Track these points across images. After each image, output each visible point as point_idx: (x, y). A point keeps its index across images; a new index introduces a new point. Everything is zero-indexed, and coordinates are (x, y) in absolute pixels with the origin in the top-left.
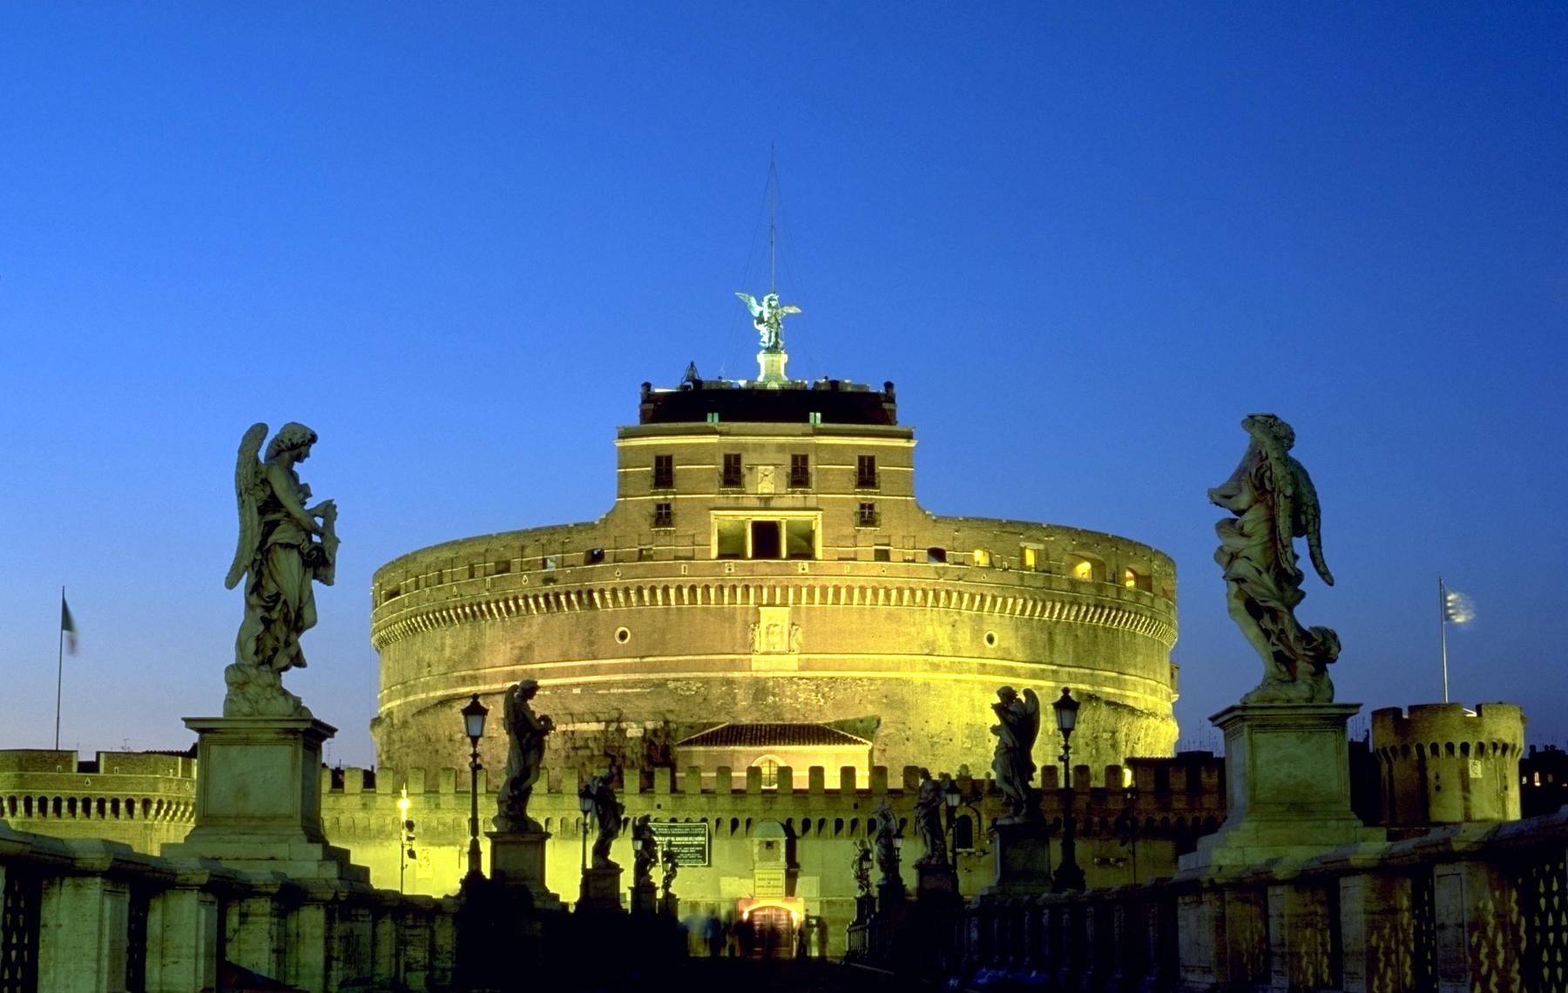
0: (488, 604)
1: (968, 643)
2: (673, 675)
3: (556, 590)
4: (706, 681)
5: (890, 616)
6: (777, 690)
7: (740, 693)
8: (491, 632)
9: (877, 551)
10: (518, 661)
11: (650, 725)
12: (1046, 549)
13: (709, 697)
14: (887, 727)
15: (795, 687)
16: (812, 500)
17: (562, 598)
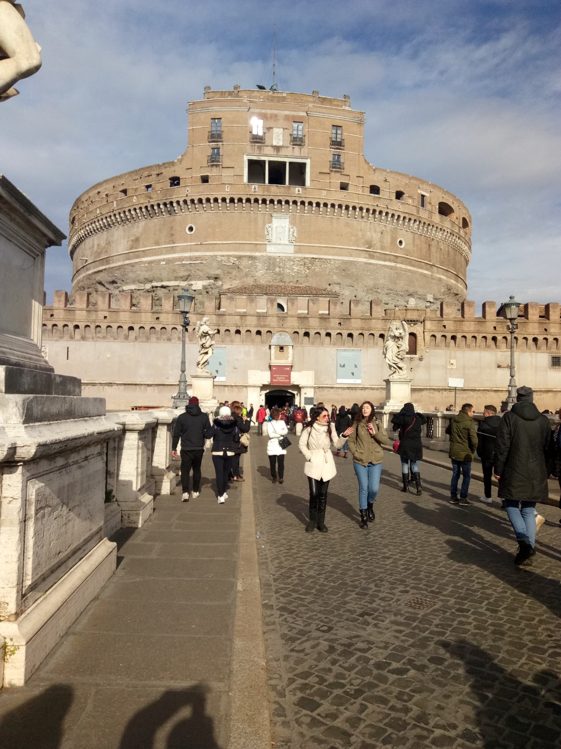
0: (115, 215)
1: (389, 244)
2: (220, 253)
3: (152, 203)
4: (239, 257)
5: (347, 225)
6: (281, 265)
7: (259, 265)
8: (118, 232)
9: (341, 183)
10: (131, 249)
11: (206, 282)
12: (430, 197)
13: (241, 267)
14: (343, 289)
15: (292, 263)
16: (305, 150)
17: (156, 208)
